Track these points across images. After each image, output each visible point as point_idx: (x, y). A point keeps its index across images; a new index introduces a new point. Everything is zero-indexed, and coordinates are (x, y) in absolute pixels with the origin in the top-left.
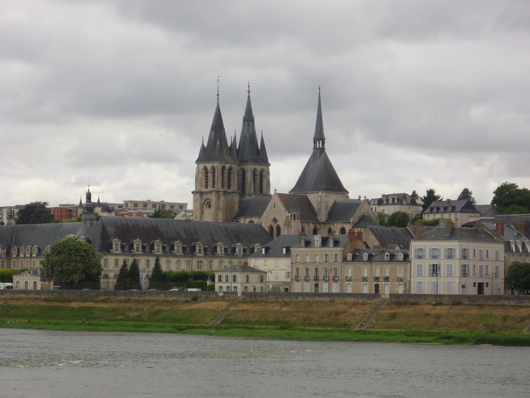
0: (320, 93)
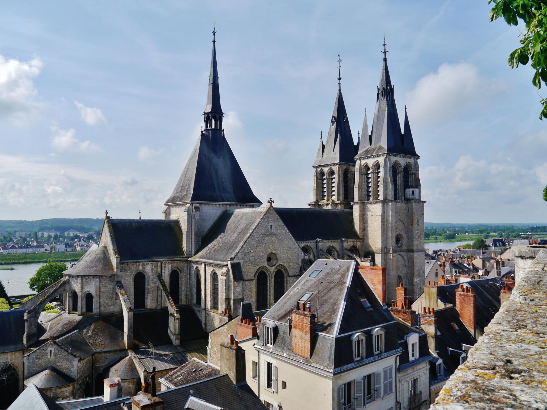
0: (214, 42)
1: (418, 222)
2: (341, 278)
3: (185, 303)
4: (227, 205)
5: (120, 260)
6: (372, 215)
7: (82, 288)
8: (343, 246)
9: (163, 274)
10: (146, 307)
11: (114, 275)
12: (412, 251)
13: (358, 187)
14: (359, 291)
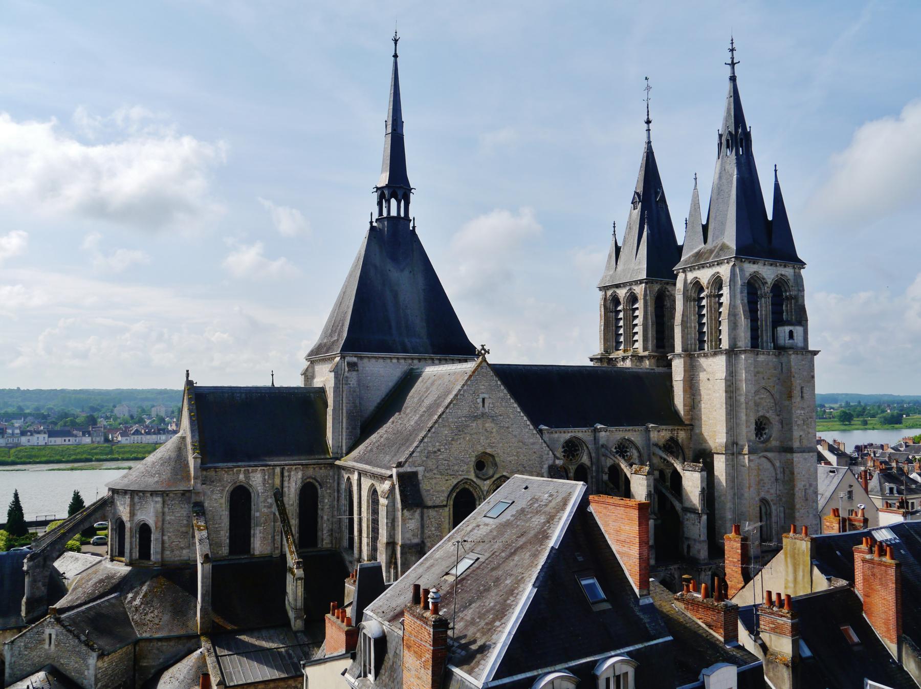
0: (396, 56)
1: (802, 392)
2: (544, 524)
3: (329, 546)
4: (412, 359)
5: (202, 463)
6: (708, 379)
7: (132, 514)
8: (649, 439)
9: (286, 489)
10: (252, 551)
11: (189, 491)
12: (790, 450)
13: (682, 324)
14: (580, 559)
